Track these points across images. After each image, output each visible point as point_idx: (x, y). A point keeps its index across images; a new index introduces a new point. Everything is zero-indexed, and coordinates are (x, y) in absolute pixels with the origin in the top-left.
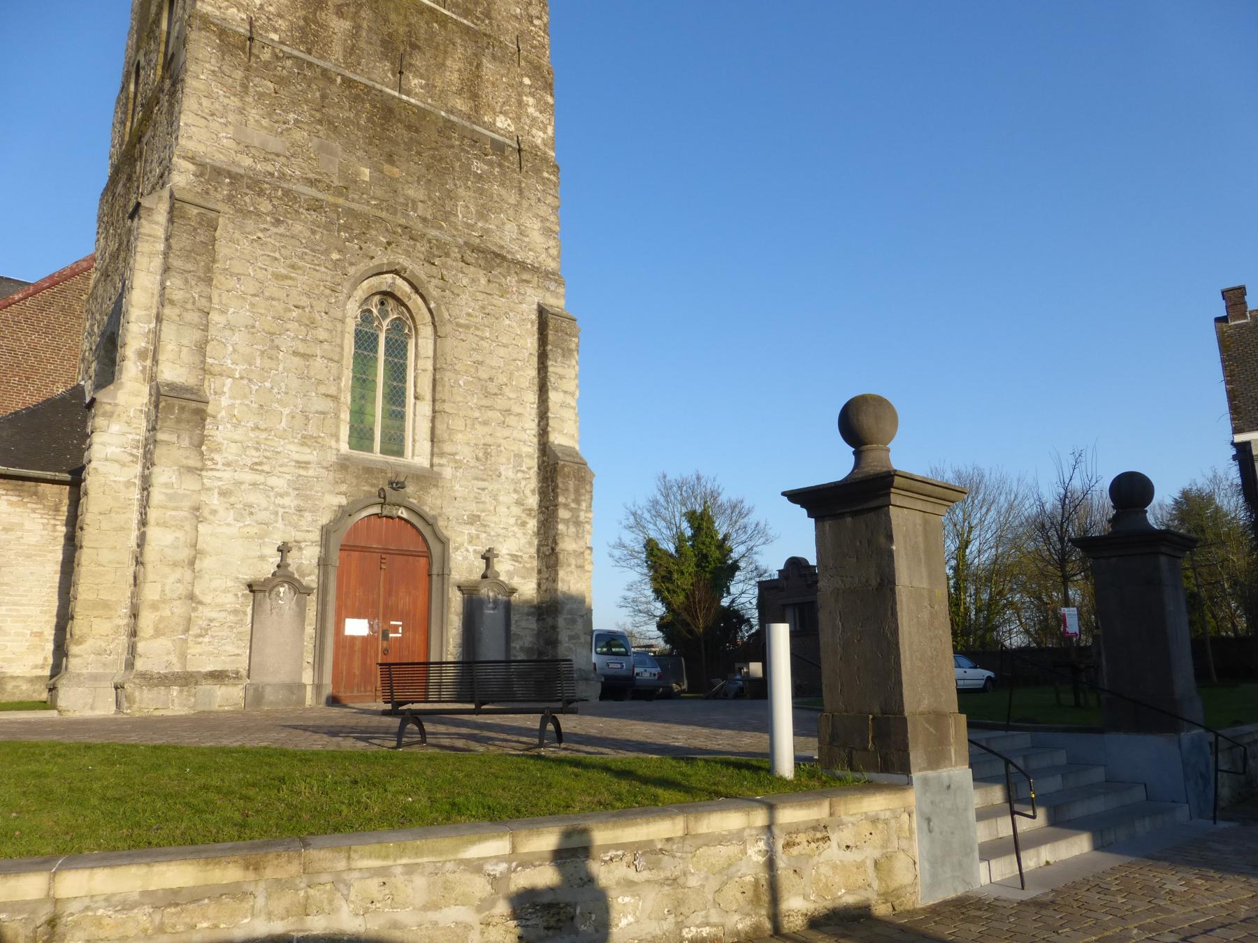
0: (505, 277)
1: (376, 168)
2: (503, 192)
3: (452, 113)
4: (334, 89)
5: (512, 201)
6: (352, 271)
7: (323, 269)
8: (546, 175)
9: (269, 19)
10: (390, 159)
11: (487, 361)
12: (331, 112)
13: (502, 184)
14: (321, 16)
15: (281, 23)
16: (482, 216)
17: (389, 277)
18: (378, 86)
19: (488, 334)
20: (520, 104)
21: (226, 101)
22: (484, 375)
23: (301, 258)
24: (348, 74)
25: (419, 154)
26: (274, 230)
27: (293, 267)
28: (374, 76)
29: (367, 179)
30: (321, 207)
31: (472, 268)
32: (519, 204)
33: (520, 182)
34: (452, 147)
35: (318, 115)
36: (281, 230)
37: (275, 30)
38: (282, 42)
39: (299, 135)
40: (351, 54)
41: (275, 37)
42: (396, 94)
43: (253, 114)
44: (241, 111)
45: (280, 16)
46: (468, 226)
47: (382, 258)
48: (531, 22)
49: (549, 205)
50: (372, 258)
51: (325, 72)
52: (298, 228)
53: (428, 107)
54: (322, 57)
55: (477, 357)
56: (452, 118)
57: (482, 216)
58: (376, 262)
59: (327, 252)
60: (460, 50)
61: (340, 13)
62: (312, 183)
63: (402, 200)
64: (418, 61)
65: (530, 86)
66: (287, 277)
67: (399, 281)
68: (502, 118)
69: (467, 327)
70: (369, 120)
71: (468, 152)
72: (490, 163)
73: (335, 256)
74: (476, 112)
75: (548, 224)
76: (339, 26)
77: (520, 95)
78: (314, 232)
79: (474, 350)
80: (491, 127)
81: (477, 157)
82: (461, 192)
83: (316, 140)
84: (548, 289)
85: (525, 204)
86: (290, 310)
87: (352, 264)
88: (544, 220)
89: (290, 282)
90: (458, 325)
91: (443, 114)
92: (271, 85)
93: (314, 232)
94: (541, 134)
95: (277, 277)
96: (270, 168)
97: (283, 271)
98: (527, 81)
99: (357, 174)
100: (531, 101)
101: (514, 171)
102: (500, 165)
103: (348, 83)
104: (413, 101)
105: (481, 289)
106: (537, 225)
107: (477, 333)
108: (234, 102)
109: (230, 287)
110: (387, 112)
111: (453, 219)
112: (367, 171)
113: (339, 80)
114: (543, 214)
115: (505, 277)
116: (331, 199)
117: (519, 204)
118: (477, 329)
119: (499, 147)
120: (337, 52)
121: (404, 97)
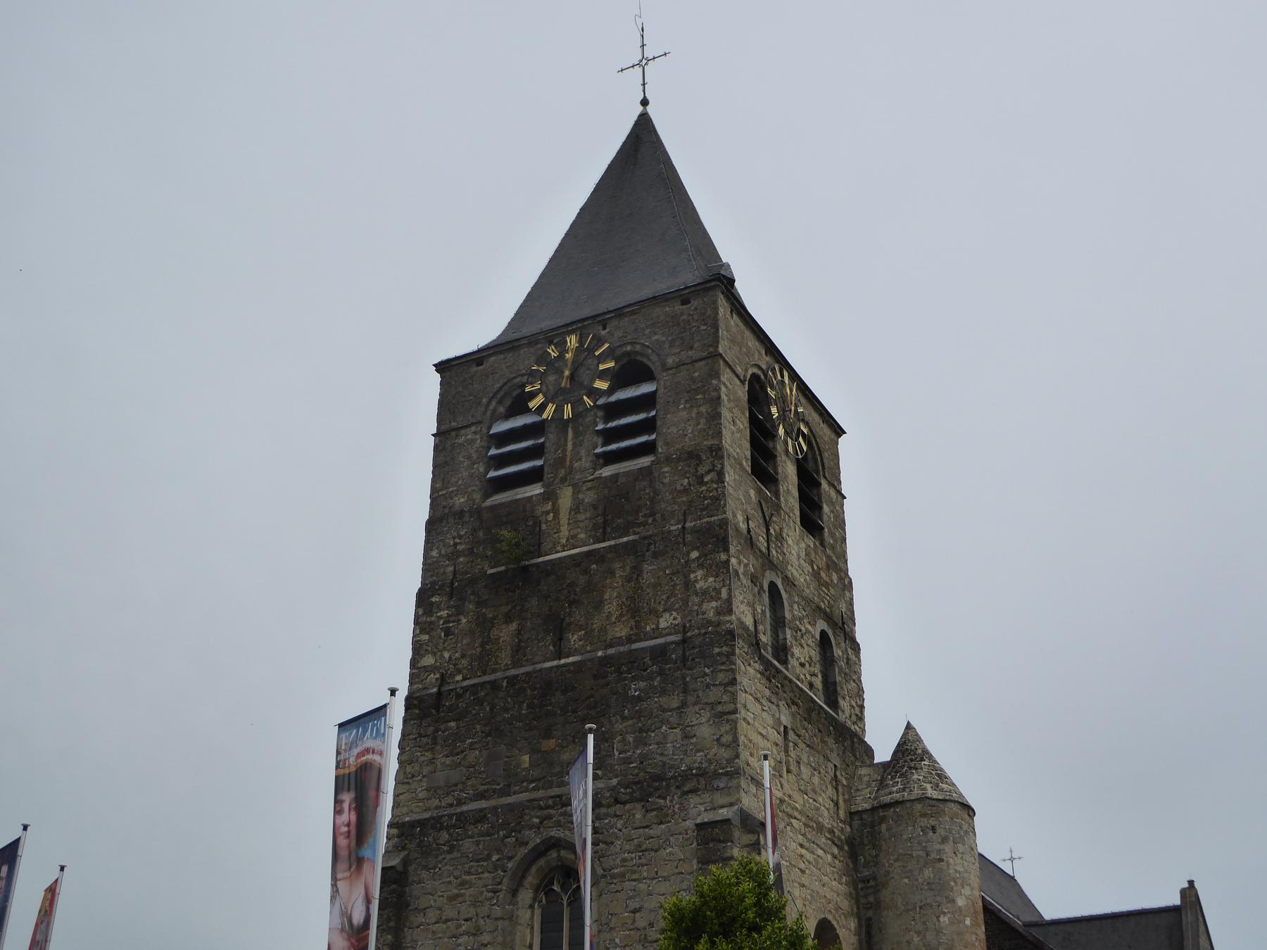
0: (665, 798)
1: (534, 751)
2: (663, 700)
3: (611, 646)
4: (501, 694)
5: (675, 704)
6: (510, 865)
7: (486, 875)
8: (717, 650)
9: (455, 665)
10: (548, 734)
11: (646, 905)
12: (498, 718)
13: (663, 692)
14: (494, 633)
15: (464, 662)
16: (641, 742)
17: (553, 854)
18: (538, 666)
19: (645, 874)
20: (688, 584)
21: (422, 759)
22: (641, 923)
23: (469, 873)
24: (513, 672)
25: (574, 711)
26: (448, 857)
27: (462, 884)
28: (536, 659)
29: (527, 765)
30: (485, 816)
31: (628, 806)
32: (684, 704)
33: (684, 678)
34: (607, 684)
35: (487, 729)
36: (455, 854)
37: (459, 672)
38: (464, 679)
39: (472, 756)
40: (517, 651)
41: (459, 678)
42: (555, 663)
43: (441, 760)
44: (431, 762)
45: (463, 656)
46: (627, 761)
47: (535, 840)
48: (702, 483)
49: (720, 684)
50: (527, 843)
51: (494, 685)
52: (468, 845)
53: (588, 656)
54: (494, 671)
55: (634, 904)
56: (611, 651)
57: (641, 742)
58: (530, 846)
59: (489, 857)
60: (619, 573)
61: (508, 619)
62: (481, 796)
63: (558, 769)
64: (578, 616)
65: (697, 558)
66: (458, 896)
67: (563, 853)
68: (667, 615)
69: (622, 875)
70: (528, 707)
71: (625, 679)
72: (650, 678)
73: (495, 858)
74: (637, 627)
75: (720, 708)
76: (505, 633)
77: (686, 576)
78: (478, 843)
79: (630, 898)
80: (658, 632)
81: (634, 678)
82: (619, 726)
83: (485, 753)
84: (718, 789)
85: (691, 699)
86: (460, 926)
87: (510, 858)
88: (713, 705)
89: (460, 899)
90: (613, 877)
91: (600, 654)
92: (453, 724)
93: (478, 843)
94: (714, 604)
95: (452, 898)
96: (450, 800)
97: (455, 891)
98: (694, 554)
99: (518, 766)
100: (700, 573)
101: (678, 668)
102: (661, 673)
103: (512, 680)
104: (571, 659)
105: (638, 824)
106: (706, 714)
107: (634, 877)
108: (429, 755)
109: (416, 924)
110: (547, 685)
111: (609, 761)
112: (526, 758)
113: (505, 684)
114: (711, 700)
115: (665, 798)
116: (493, 803)
117: (684, 704)
118: (634, 872)
119: (660, 654)
120: (505, 657)
121: (563, 661)
